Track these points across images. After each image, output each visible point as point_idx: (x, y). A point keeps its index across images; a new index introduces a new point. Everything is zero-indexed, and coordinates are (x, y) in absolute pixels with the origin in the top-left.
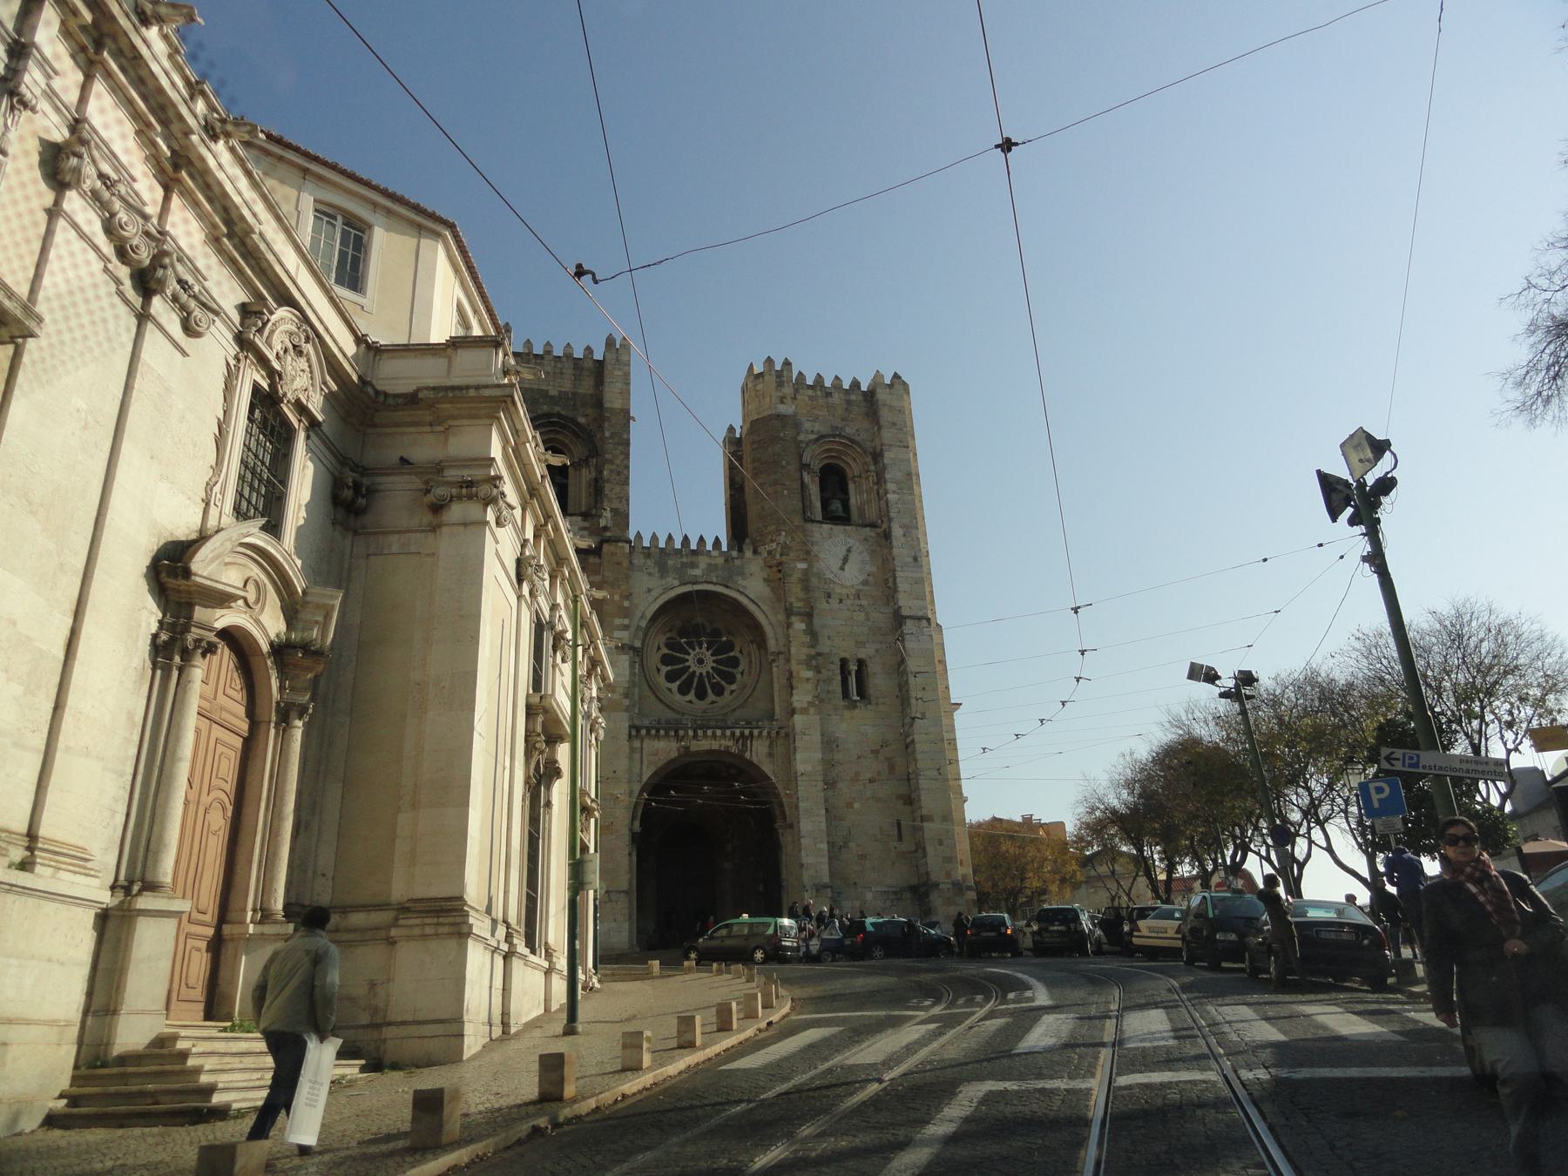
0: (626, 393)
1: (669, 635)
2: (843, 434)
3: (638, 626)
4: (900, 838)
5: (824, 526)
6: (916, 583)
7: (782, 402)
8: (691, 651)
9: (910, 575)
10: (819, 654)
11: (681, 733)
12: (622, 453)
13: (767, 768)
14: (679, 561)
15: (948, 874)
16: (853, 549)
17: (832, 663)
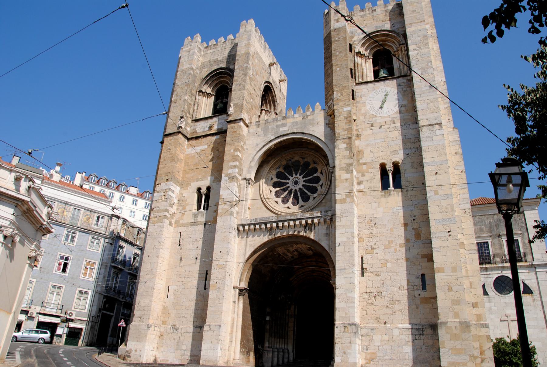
0: (248, 45)
1: (278, 170)
2: (382, 29)
3: (250, 166)
4: (424, 287)
5: (370, 85)
6: (431, 102)
7: (338, 21)
8: (290, 177)
9: (428, 98)
10: (364, 164)
11: (269, 225)
12: (242, 74)
13: (324, 243)
14: (276, 125)
15: (456, 315)
16: (389, 94)
17: (374, 168)
